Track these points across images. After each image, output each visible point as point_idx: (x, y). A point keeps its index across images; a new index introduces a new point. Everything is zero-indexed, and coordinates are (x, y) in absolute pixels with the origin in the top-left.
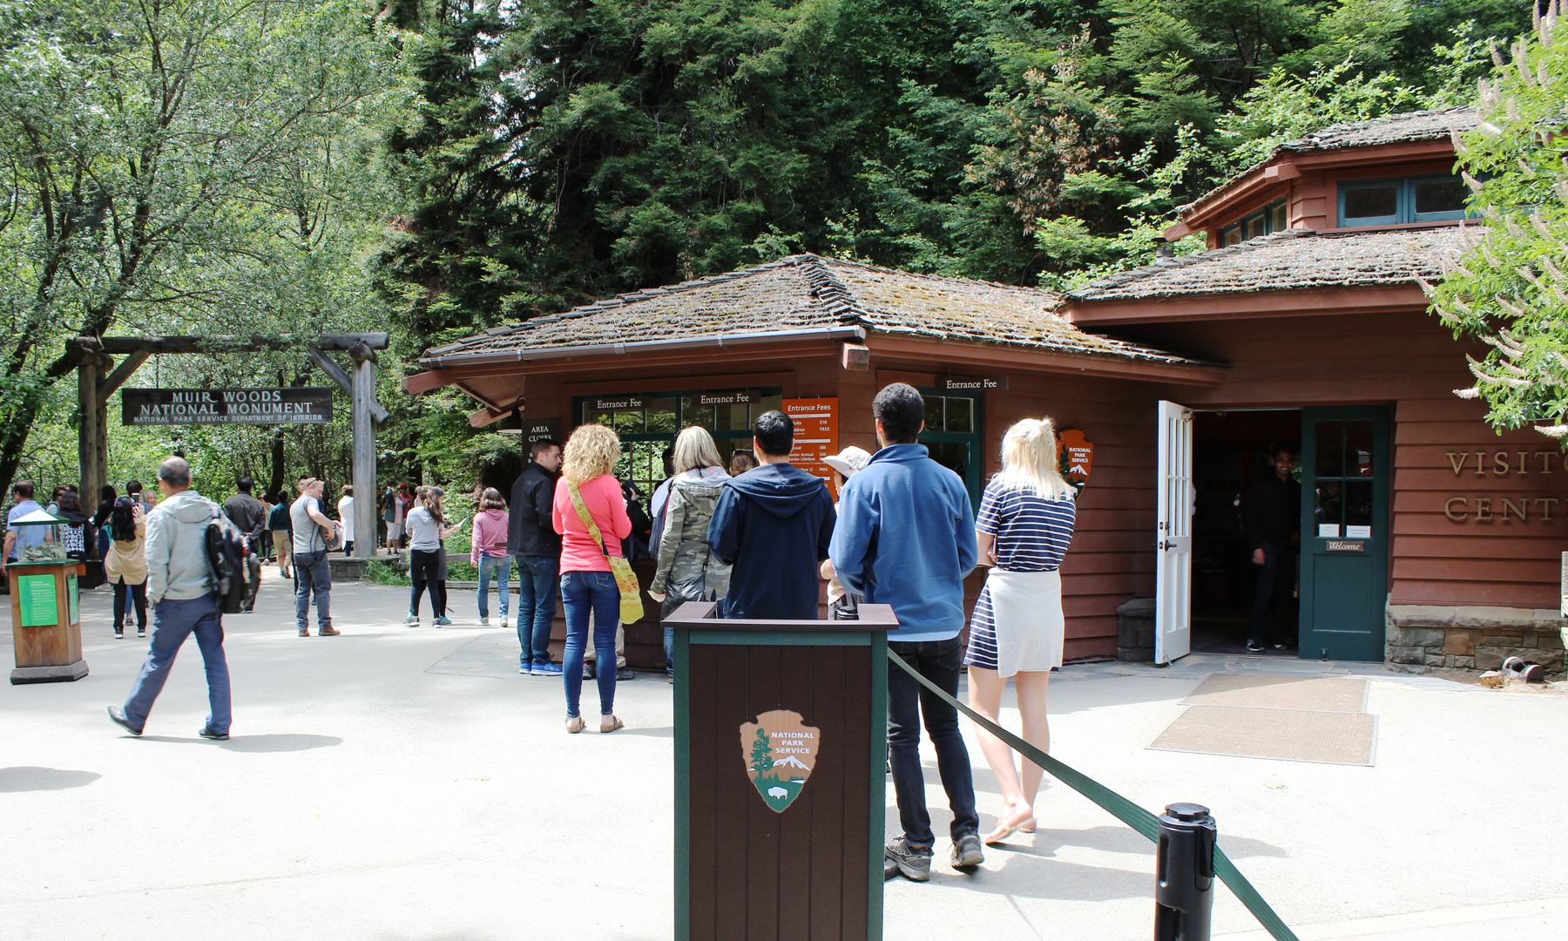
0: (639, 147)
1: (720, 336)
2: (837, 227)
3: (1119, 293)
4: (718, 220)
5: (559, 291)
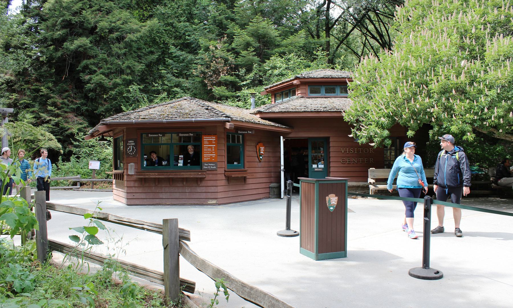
0: (95, 57)
1: (193, 119)
2: (156, 85)
3: (270, 111)
4: (118, 81)
5: (65, 98)
